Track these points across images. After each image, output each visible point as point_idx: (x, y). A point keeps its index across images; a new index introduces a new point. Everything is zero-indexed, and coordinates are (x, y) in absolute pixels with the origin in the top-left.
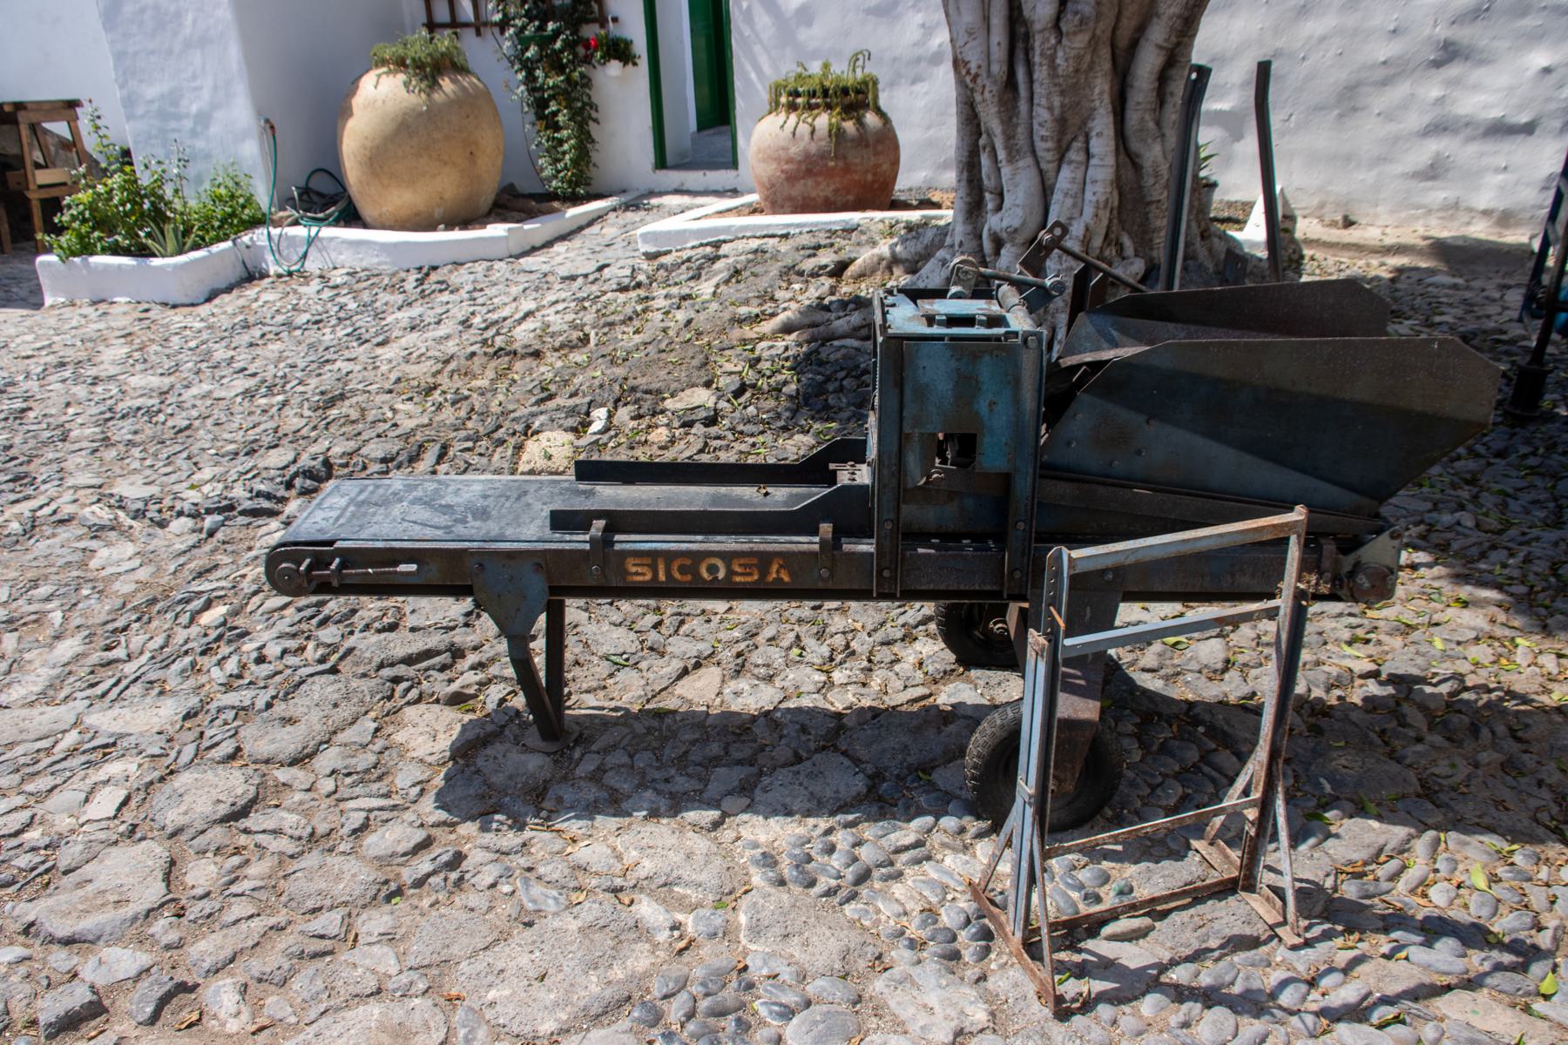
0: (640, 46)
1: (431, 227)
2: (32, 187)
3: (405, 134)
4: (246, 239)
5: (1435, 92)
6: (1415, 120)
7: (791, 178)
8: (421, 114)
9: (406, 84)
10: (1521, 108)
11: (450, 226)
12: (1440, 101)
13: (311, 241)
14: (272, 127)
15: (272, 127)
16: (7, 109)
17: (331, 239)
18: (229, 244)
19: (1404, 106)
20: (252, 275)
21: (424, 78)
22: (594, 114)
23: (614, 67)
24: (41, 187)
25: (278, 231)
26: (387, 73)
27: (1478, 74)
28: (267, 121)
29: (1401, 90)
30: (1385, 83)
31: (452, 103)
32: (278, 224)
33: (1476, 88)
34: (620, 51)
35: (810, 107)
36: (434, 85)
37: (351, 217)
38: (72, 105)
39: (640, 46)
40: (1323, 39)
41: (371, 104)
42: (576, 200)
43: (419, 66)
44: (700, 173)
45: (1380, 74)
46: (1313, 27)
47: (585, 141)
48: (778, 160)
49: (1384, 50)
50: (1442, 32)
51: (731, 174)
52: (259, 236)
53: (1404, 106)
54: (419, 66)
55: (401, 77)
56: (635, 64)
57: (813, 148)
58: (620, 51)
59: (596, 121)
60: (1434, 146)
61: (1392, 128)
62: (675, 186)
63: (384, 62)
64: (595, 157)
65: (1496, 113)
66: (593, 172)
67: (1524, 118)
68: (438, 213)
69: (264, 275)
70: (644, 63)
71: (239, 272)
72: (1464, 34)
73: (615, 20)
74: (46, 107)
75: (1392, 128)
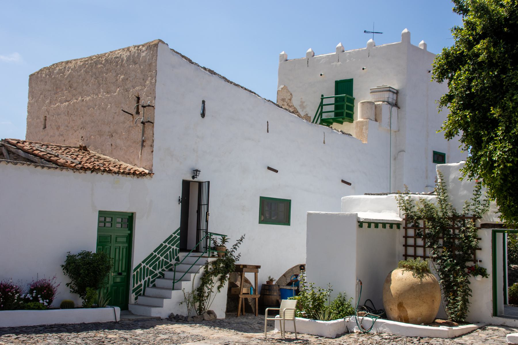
0: (489, 270)
1: (419, 324)
2: (241, 293)
3: (412, 290)
4: (347, 319)
8: (418, 285)
9: (413, 275)
11: (426, 324)
13: (374, 322)
14: (361, 283)
15: (361, 283)
16: (241, 267)
17: (382, 323)
18: (343, 320)
20: (348, 332)
21: (419, 273)
22: (470, 293)
23: (479, 277)
24: (243, 294)
25: (361, 318)
26: (406, 270)
28: (360, 281)
31: (428, 284)
32: (359, 315)
34: (482, 272)
36: (422, 276)
37: (385, 316)
38: (258, 267)
39: (489, 270)
41: (400, 280)
42: (461, 323)
43: (417, 269)
44: (513, 320)
47: (465, 301)
52: (351, 319)
54: (417, 269)
55: (411, 273)
56: (487, 277)
58: (482, 272)
59: (470, 295)
62: (501, 323)
63: (404, 267)
64: (469, 309)
66: (468, 313)
68: (419, 319)
69: (353, 332)
70: (490, 277)
71: (343, 330)
73: (480, 261)
74: (251, 267)
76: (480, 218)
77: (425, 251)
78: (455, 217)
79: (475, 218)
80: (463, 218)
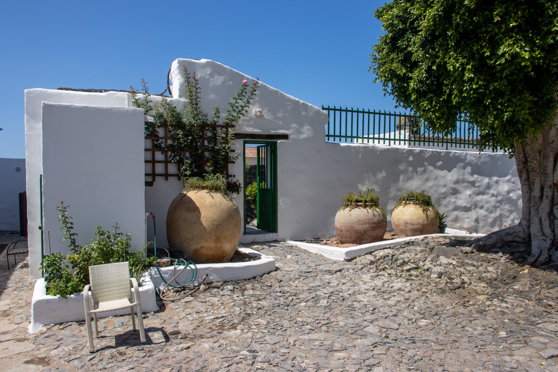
5: (453, 200)
6: (451, 207)
7: (374, 229)
10: (468, 203)
12: (455, 202)
19: (449, 203)
27: (459, 196)
29: (448, 199)
30: (445, 198)
33: (460, 199)
35: (371, 206)
40: (432, 187)
44: (263, 235)
45: (443, 196)
46: (430, 184)
48: (369, 223)
49: (443, 190)
50: (452, 186)
51: (275, 234)
53: (449, 203)
57: (380, 219)
60: (456, 213)
61: (447, 209)
65: (464, 205)
67: (469, 206)
72: (457, 186)
73: (234, 176)
75: (447, 209)
76: (233, 126)
77: (166, 168)
78: (204, 126)
79: (227, 126)
80: (214, 126)
